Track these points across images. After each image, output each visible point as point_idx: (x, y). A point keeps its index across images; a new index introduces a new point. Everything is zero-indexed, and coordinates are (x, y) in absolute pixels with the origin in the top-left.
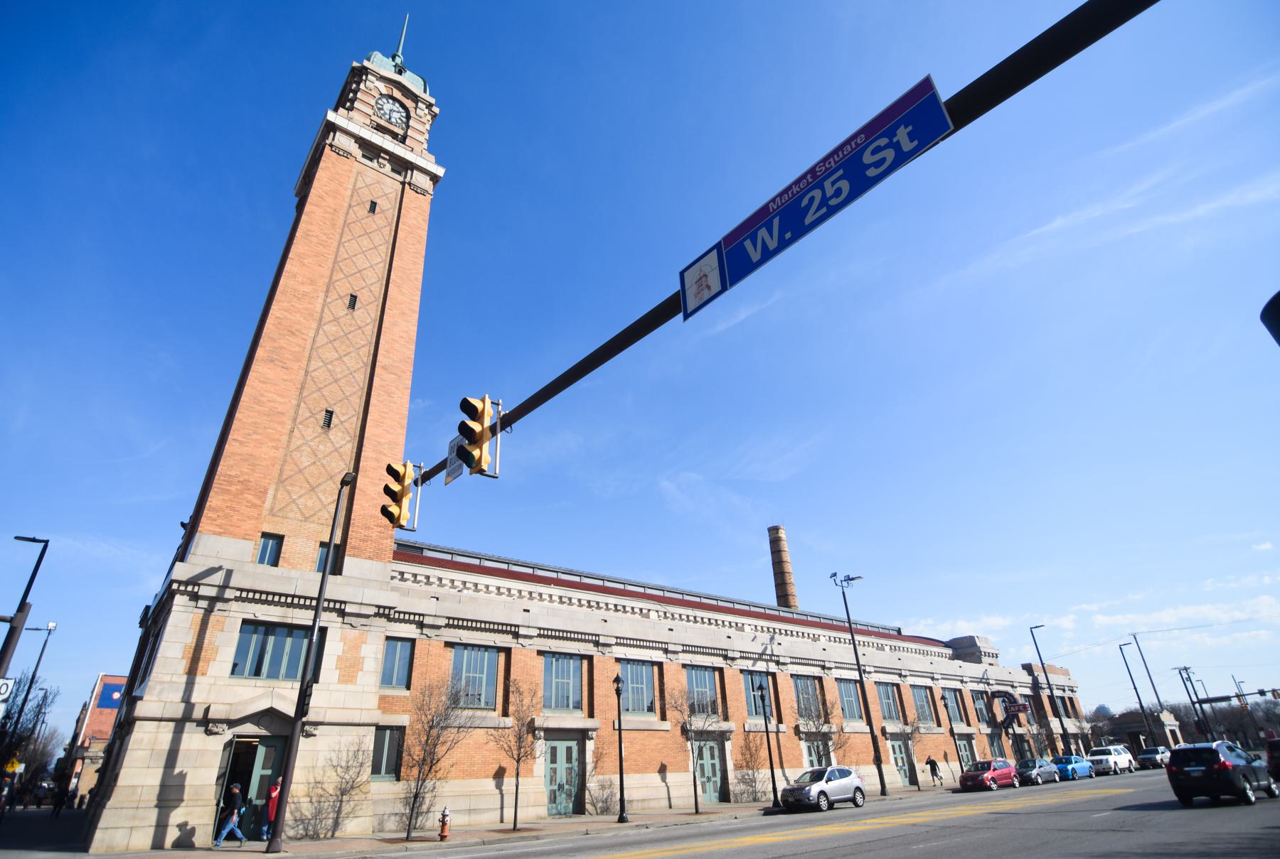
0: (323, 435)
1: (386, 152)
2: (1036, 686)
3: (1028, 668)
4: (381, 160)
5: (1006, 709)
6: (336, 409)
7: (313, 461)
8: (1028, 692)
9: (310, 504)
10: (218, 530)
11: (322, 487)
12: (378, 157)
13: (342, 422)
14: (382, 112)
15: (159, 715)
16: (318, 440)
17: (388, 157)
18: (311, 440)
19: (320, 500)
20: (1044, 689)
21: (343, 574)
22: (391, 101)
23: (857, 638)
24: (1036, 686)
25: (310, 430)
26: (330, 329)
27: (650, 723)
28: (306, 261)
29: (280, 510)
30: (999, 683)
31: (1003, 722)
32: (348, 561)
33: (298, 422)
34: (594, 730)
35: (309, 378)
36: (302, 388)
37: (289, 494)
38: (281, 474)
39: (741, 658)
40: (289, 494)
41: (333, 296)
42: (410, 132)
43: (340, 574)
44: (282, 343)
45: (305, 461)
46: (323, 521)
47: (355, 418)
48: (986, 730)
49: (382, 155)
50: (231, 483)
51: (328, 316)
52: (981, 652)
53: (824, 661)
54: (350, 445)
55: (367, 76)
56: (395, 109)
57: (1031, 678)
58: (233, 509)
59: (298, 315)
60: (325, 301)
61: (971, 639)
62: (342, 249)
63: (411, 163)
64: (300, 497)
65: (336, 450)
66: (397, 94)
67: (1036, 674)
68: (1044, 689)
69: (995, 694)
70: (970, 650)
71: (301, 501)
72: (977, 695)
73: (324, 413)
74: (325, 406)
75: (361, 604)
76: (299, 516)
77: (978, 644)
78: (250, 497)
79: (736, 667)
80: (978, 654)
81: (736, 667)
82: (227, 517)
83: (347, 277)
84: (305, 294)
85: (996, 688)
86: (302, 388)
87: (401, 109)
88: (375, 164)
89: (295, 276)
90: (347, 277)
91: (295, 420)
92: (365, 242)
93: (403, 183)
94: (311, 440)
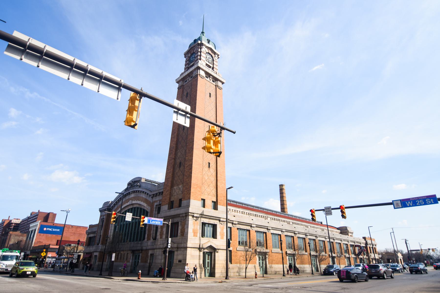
0: (209, 170)
1: (212, 76)
2: (366, 244)
3: (364, 238)
4: (210, 78)
5: (359, 250)
7: (208, 178)
8: (364, 245)
10: (194, 198)
11: (210, 185)
12: (210, 77)
13: (212, 166)
15: (191, 247)
16: (208, 172)
17: (212, 77)
18: (207, 172)
19: (211, 189)
20: (368, 245)
21: (218, 210)
22: (208, 54)
23: (329, 229)
24: (366, 244)
25: (206, 169)
27: (278, 251)
29: (203, 192)
30: (357, 242)
31: (358, 254)
32: (219, 206)
33: (204, 166)
34: (268, 252)
35: (204, 153)
36: (203, 156)
37: (204, 187)
38: (202, 182)
39: (298, 234)
40: (204, 187)
42: (215, 66)
43: (217, 210)
45: (206, 178)
46: (212, 195)
47: (214, 165)
48: (353, 256)
49: (211, 76)
52: (348, 232)
53: (316, 235)
54: (214, 173)
55: (203, 46)
56: (210, 57)
57: (365, 241)
58: (196, 192)
60: (204, 128)
61: (346, 227)
63: (218, 79)
64: (207, 188)
65: (212, 174)
66: (210, 52)
67: (367, 240)
68: (368, 245)
69: (356, 246)
70: (345, 231)
71: (207, 189)
72: (352, 246)
73: (208, 163)
74: (208, 161)
75: (223, 218)
76: (207, 194)
77: (348, 229)
79: (296, 236)
80: (348, 232)
81: (296, 236)
85: (356, 244)
86: (203, 156)
87: (211, 57)
88: (208, 79)
91: (203, 166)
93: (216, 86)
94: (207, 172)
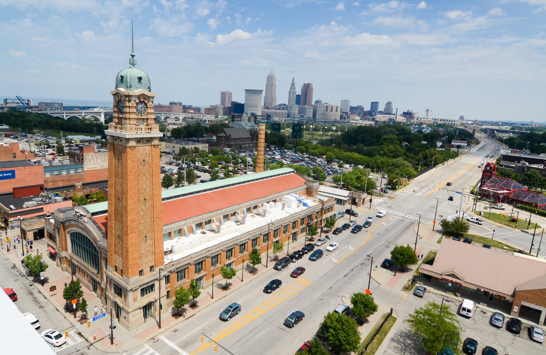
6: (147, 235)
9: (146, 260)
14: (138, 111)
26: (142, 213)
28: (132, 197)
41: (140, 202)
44: (133, 226)
50: (131, 266)
51: (140, 210)
59: (134, 216)
62: (139, 185)
65: (149, 245)
78: (136, 266)
82: (133, 273)
83: (142, 194)
84: (134, 208)
89: (131, 204)
90: (142, 194)
92: (145, 178)
